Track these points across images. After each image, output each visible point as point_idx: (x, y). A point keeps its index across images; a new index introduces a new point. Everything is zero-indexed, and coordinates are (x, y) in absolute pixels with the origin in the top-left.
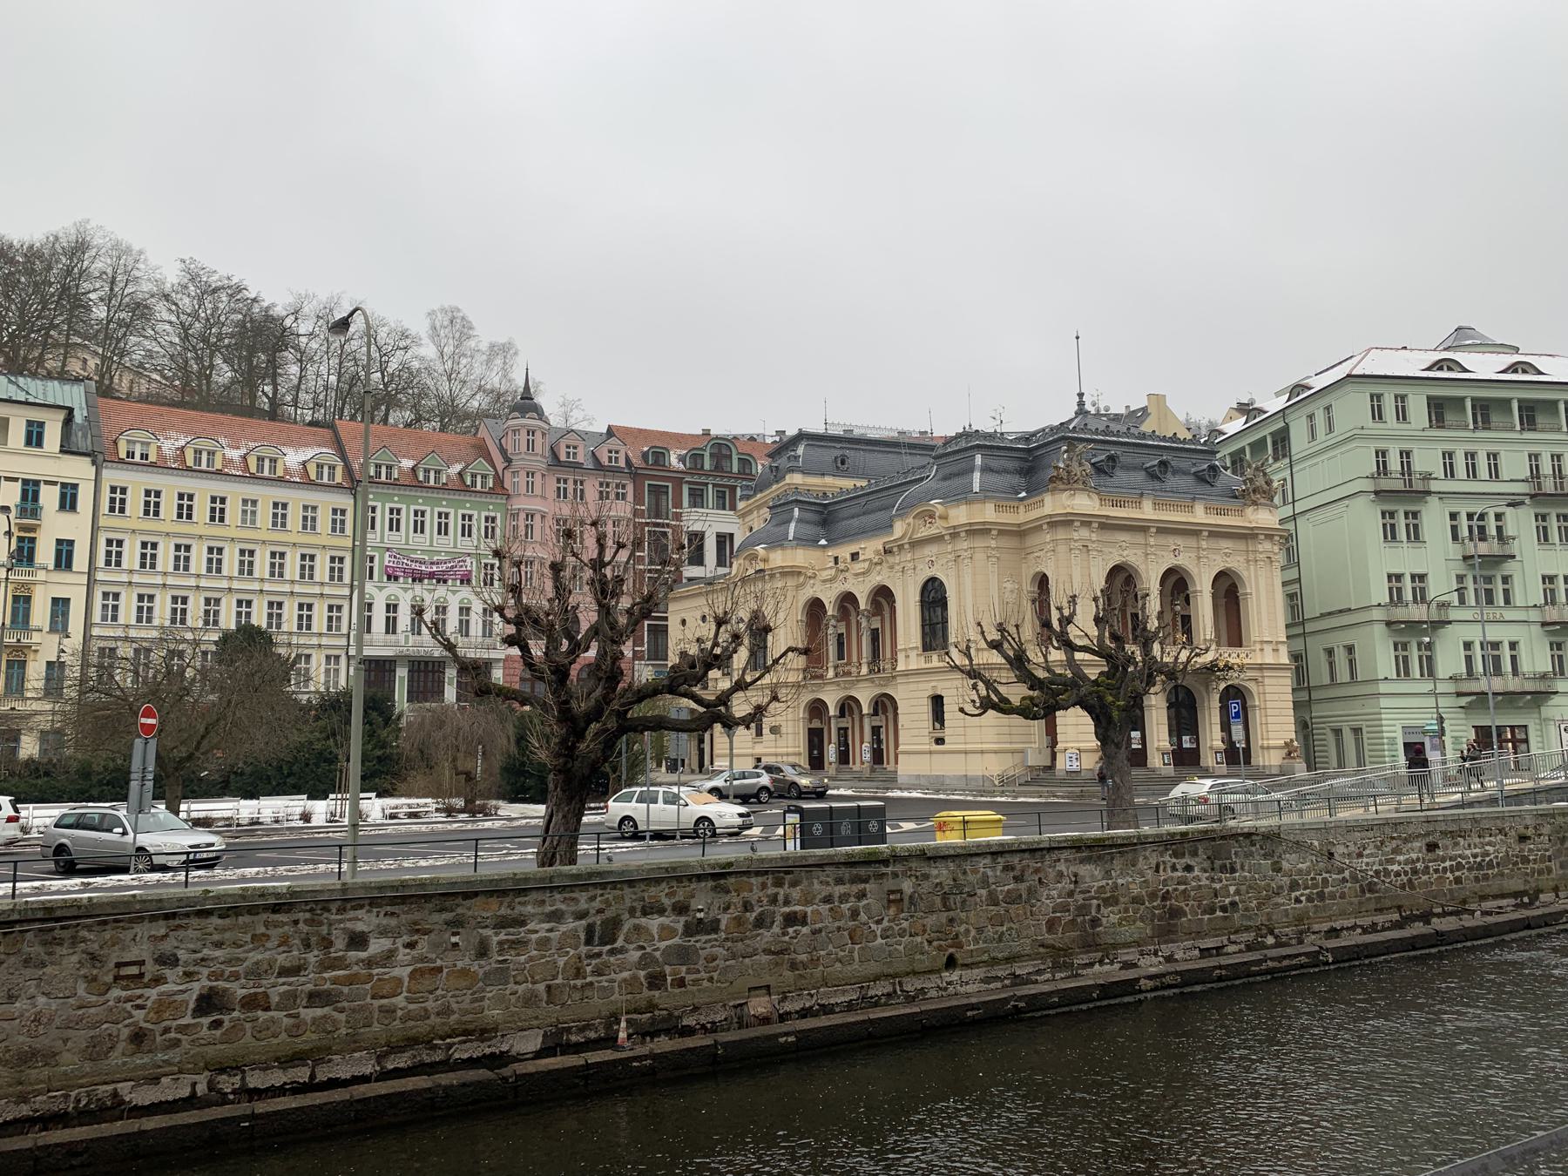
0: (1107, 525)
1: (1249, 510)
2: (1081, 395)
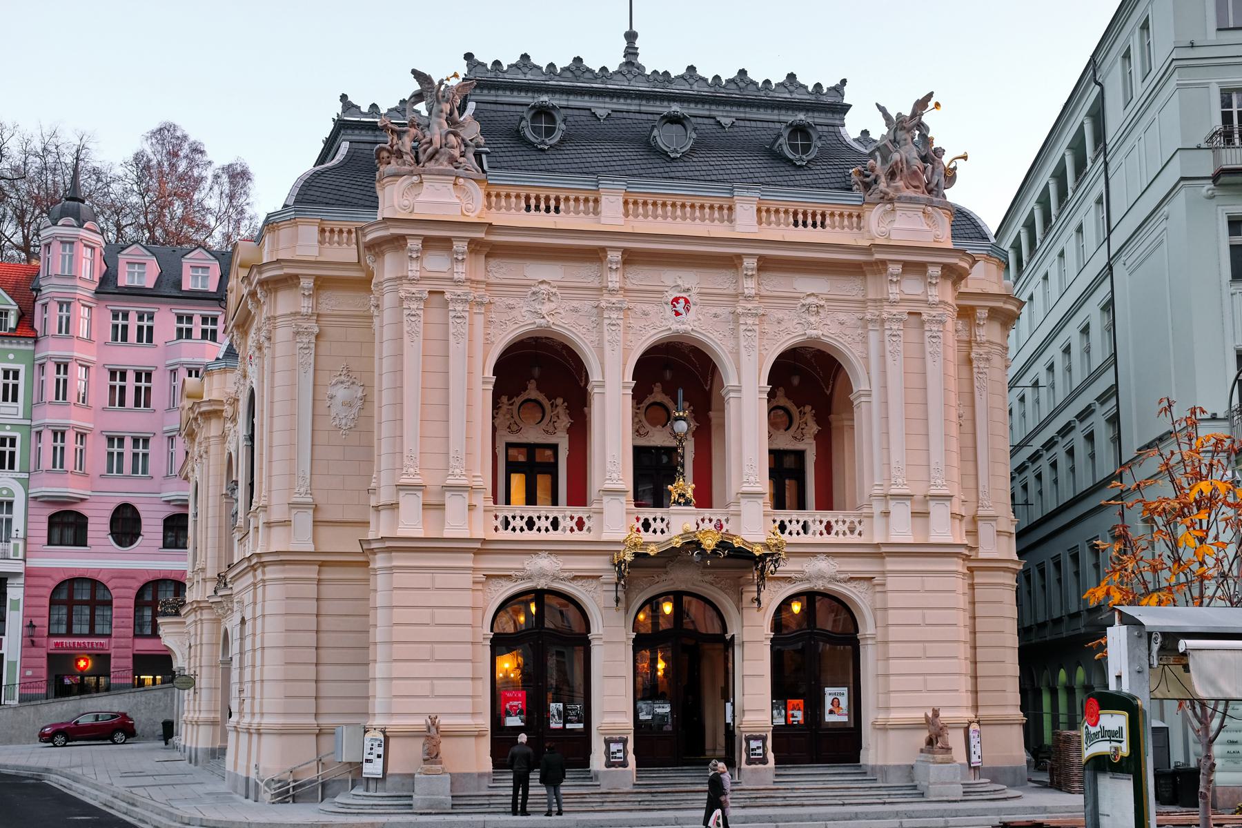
0: (490, 247)
1: (874, 216)
2: (631, 36)
